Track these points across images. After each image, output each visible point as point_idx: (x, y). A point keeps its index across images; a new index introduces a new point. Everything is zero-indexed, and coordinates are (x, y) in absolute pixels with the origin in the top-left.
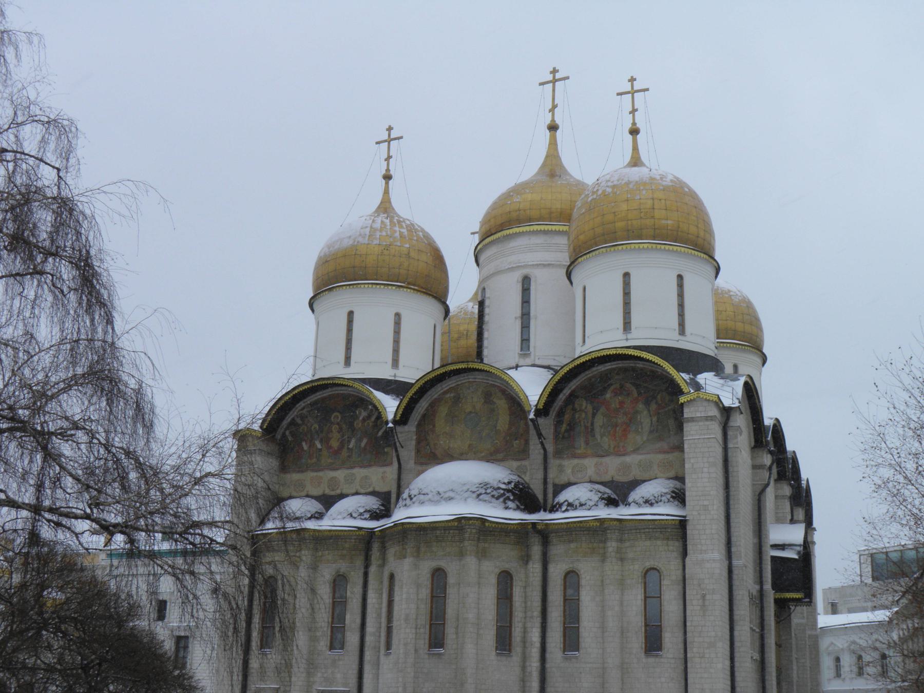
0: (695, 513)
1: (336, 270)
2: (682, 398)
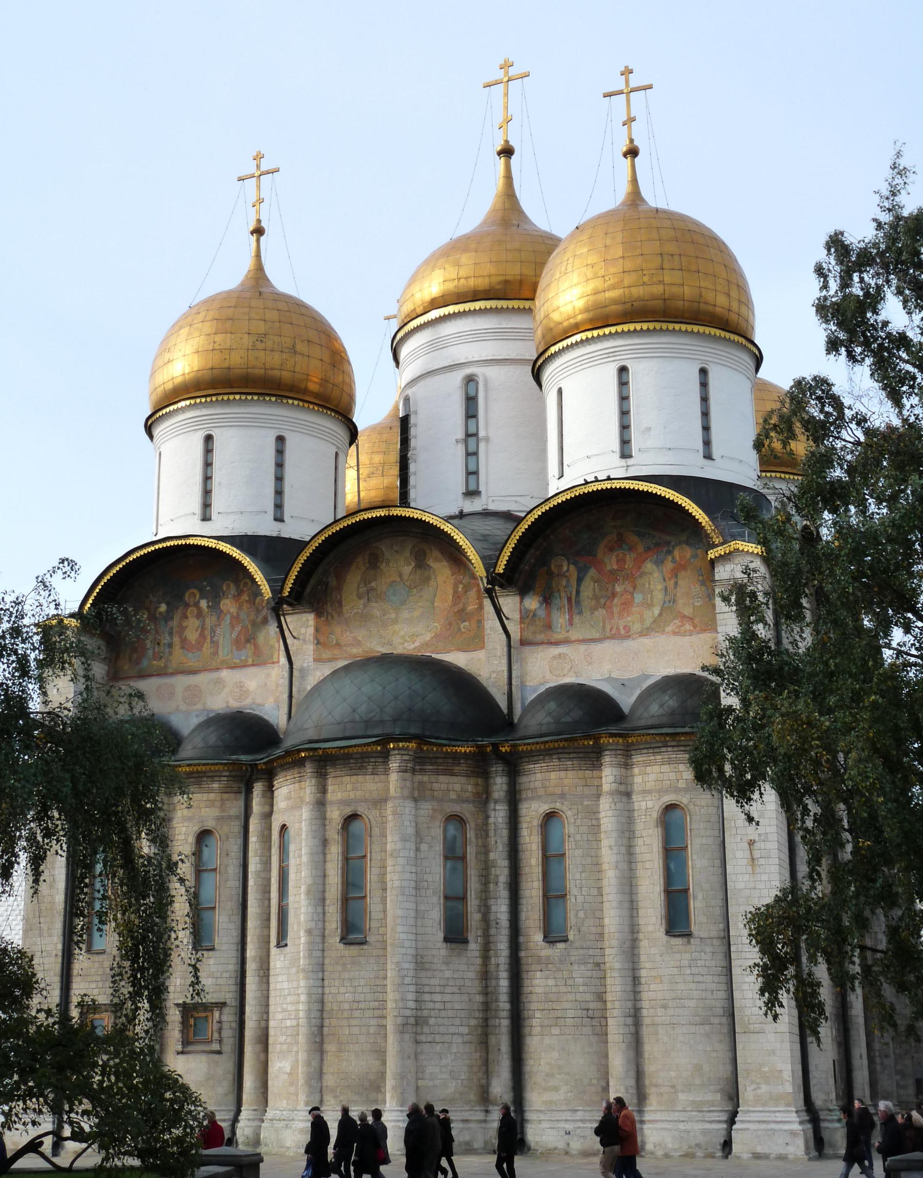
1: (184, 374)
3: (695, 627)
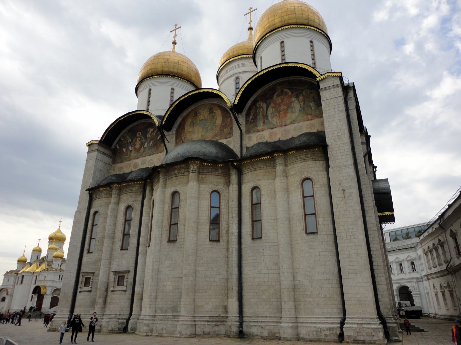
0: (332, 141)
2: (318, 78)
3: (312, 117)
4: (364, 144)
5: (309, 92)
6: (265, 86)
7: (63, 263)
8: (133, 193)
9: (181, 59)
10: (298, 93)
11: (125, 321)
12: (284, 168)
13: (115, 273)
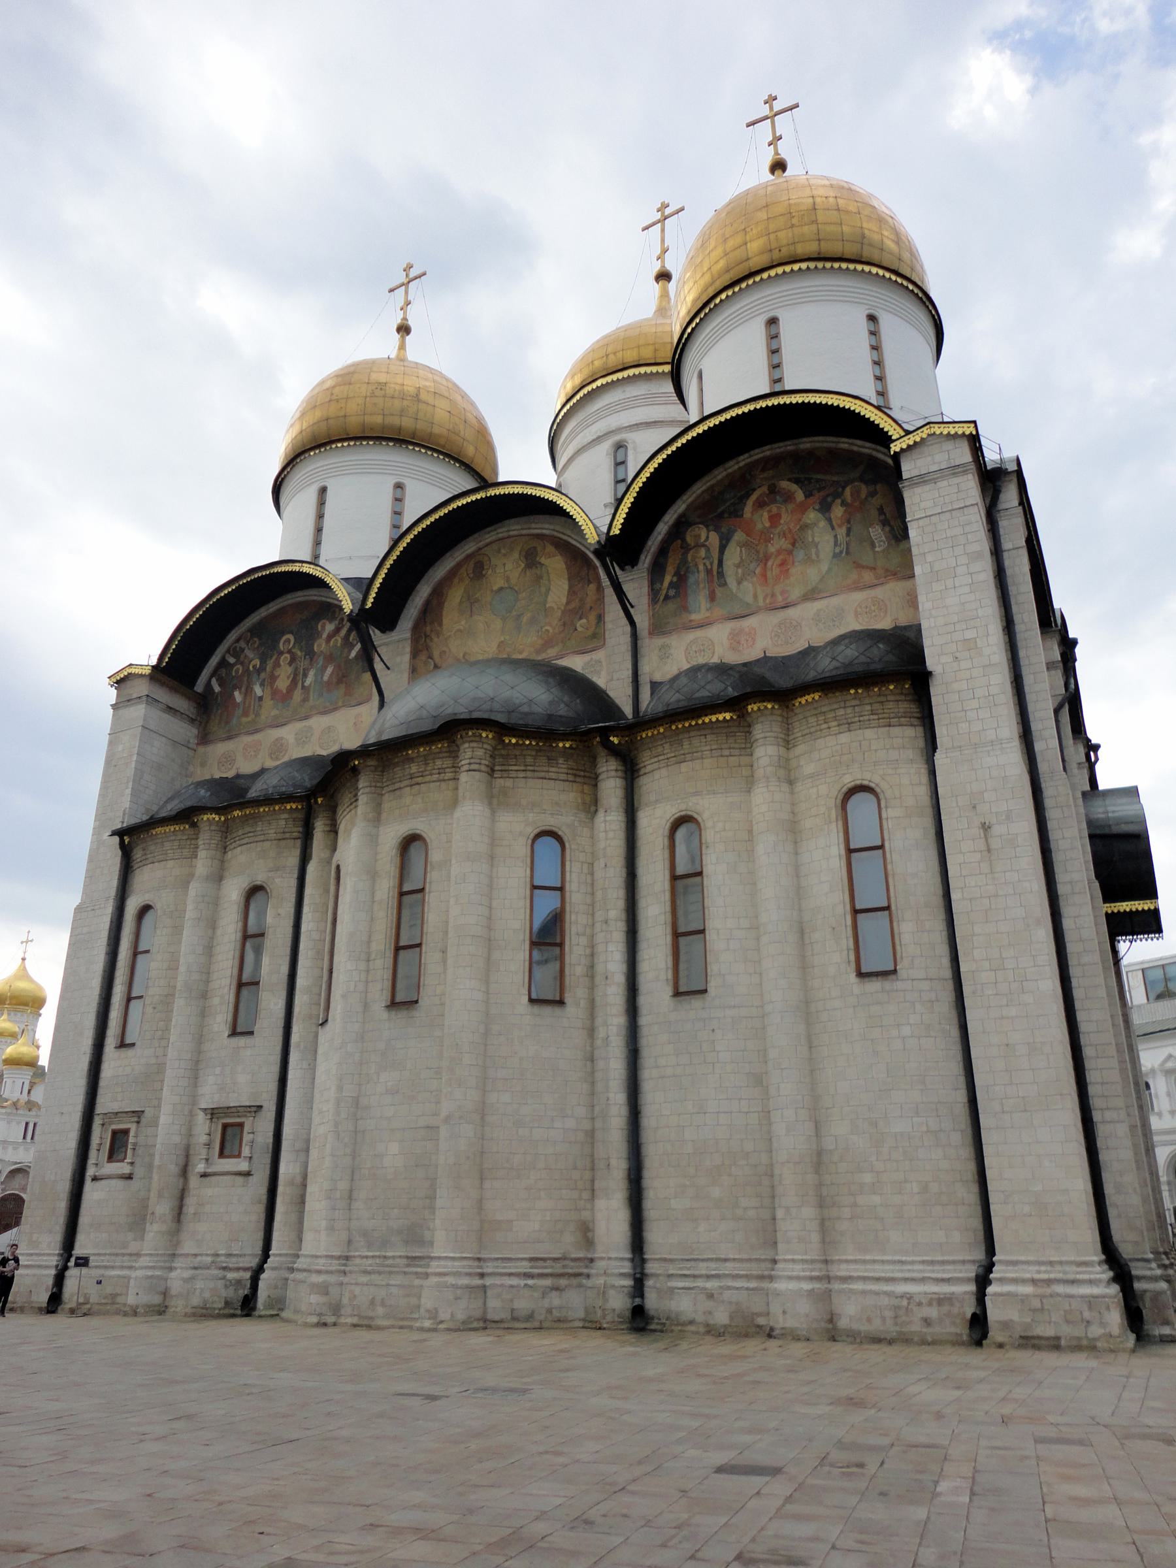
2: (897, 443)
4: (1056, 668)
5: (864, 490)
6: (716, 472)
7: (36, 1080)
8: (267, 844)
9: (428, 384)
10: (828, 495)
11: (248, 1275)
12: (782, 750)
13: (212, 1114)
